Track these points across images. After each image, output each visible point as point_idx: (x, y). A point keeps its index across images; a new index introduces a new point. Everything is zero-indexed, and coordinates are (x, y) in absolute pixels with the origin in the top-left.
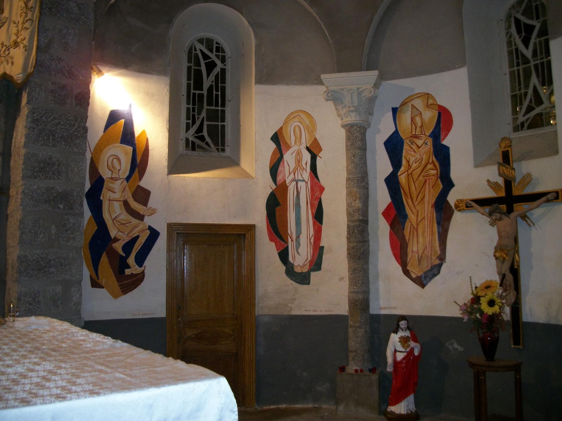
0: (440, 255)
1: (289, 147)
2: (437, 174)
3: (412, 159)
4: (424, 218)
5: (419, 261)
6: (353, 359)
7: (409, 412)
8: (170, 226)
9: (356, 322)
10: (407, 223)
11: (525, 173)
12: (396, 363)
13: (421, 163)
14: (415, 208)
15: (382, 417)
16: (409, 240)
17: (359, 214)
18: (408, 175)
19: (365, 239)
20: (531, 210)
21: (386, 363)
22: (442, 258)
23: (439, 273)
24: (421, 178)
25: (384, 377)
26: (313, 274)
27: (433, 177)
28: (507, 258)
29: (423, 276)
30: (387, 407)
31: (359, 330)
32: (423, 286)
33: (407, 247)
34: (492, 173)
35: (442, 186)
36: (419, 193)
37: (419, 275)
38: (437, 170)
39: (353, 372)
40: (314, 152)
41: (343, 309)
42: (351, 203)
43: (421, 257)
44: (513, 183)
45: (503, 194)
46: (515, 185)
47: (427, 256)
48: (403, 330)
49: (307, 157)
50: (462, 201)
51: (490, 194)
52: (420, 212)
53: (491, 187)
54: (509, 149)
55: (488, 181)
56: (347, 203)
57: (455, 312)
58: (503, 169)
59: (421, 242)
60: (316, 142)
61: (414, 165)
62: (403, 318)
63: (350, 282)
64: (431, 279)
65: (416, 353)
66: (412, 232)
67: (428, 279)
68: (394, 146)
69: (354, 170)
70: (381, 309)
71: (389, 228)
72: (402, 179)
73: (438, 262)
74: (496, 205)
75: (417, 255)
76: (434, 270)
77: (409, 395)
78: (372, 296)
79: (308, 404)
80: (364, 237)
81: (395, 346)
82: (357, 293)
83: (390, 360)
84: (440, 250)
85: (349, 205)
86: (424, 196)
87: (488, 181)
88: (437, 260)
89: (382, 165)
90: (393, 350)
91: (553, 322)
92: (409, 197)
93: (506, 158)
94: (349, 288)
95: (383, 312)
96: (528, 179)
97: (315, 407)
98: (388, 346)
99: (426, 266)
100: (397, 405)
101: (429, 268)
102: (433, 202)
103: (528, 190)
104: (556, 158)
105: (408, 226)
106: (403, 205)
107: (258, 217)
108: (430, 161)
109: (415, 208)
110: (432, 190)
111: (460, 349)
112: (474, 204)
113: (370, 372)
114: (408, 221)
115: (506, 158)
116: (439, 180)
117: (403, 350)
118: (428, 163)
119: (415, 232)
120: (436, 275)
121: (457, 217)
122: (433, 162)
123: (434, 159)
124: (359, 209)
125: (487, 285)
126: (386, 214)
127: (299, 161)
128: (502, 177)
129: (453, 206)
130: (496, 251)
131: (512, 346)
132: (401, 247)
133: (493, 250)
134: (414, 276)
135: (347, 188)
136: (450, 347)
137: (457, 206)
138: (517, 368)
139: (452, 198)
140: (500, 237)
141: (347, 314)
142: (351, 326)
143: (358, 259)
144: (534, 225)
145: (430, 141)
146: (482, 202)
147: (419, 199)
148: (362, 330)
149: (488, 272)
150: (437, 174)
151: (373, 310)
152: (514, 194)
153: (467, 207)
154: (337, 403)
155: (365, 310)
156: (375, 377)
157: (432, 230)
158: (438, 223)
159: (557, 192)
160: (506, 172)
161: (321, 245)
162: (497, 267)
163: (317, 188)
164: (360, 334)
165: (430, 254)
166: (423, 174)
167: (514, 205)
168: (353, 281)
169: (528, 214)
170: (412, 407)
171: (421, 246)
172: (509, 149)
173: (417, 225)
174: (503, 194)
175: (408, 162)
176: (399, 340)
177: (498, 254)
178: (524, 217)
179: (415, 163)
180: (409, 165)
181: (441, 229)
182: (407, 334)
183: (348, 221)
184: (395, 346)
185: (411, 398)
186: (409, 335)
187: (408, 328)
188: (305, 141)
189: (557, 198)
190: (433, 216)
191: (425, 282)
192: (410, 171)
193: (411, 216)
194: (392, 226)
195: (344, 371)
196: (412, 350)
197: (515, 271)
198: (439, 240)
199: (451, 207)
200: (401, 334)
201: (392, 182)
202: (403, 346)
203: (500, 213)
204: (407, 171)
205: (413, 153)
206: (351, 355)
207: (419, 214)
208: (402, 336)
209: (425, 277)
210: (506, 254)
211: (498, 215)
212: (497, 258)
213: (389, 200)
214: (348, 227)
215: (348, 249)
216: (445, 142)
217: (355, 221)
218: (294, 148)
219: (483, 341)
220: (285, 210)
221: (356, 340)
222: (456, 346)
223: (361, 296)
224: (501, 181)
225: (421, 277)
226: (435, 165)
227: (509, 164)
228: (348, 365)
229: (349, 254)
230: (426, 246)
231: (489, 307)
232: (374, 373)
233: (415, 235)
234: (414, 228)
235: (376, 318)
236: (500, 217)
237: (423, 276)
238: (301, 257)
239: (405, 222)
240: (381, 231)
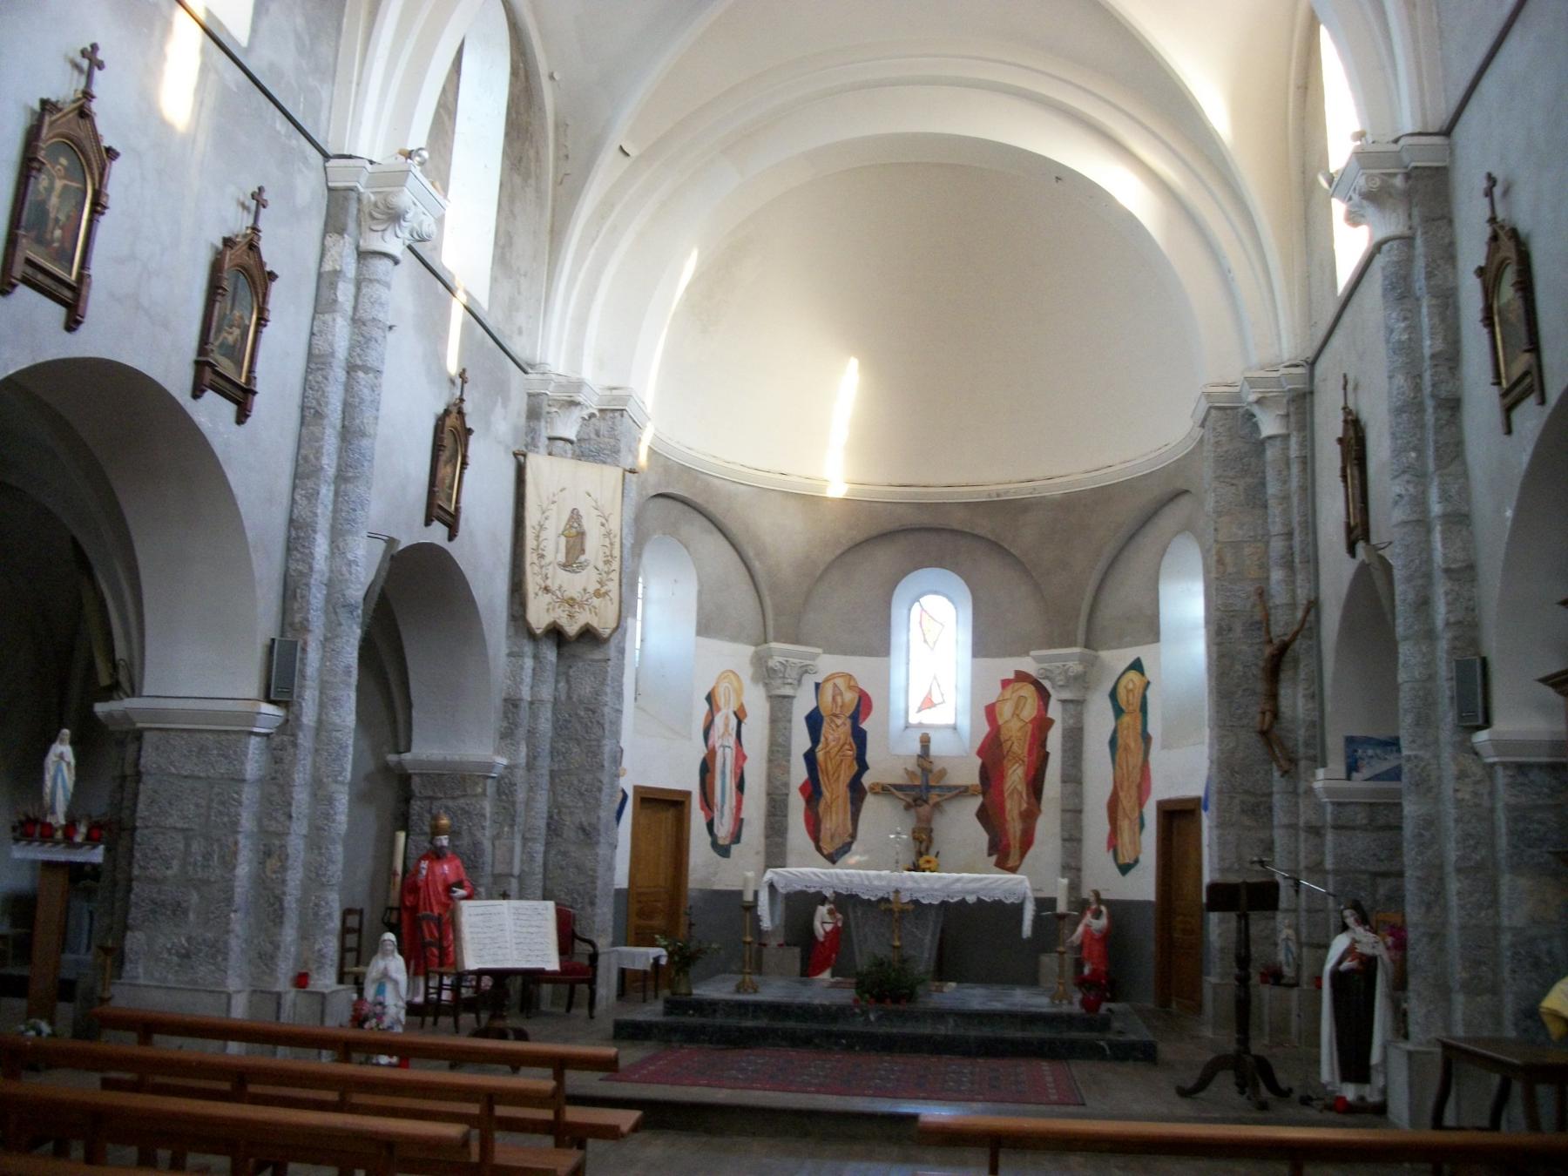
1: (719, 710)
8: (637, 789)
22: (853, 836)
26: (734, 848)
40: (740, 716)
49: (734, 721)
52: (835, 791)
59: (834, 821)
60: (742, 708)
68: (814, 722)
72: (820, 755)
89: (801, 740)
99: (838, 843)
107: (692, 784)
126: (803, 789)
127: (727, 725)
137: (872, 789)
139: (867, 780)
140: (919, 819)
145: (849, 722)
163: (740, 757)
188: (734, 706)
193: (826, 793)
201: (810, 758)
216: (864, 726)
218: (723, 711)
220: (713, 777)
238: (724, 830)
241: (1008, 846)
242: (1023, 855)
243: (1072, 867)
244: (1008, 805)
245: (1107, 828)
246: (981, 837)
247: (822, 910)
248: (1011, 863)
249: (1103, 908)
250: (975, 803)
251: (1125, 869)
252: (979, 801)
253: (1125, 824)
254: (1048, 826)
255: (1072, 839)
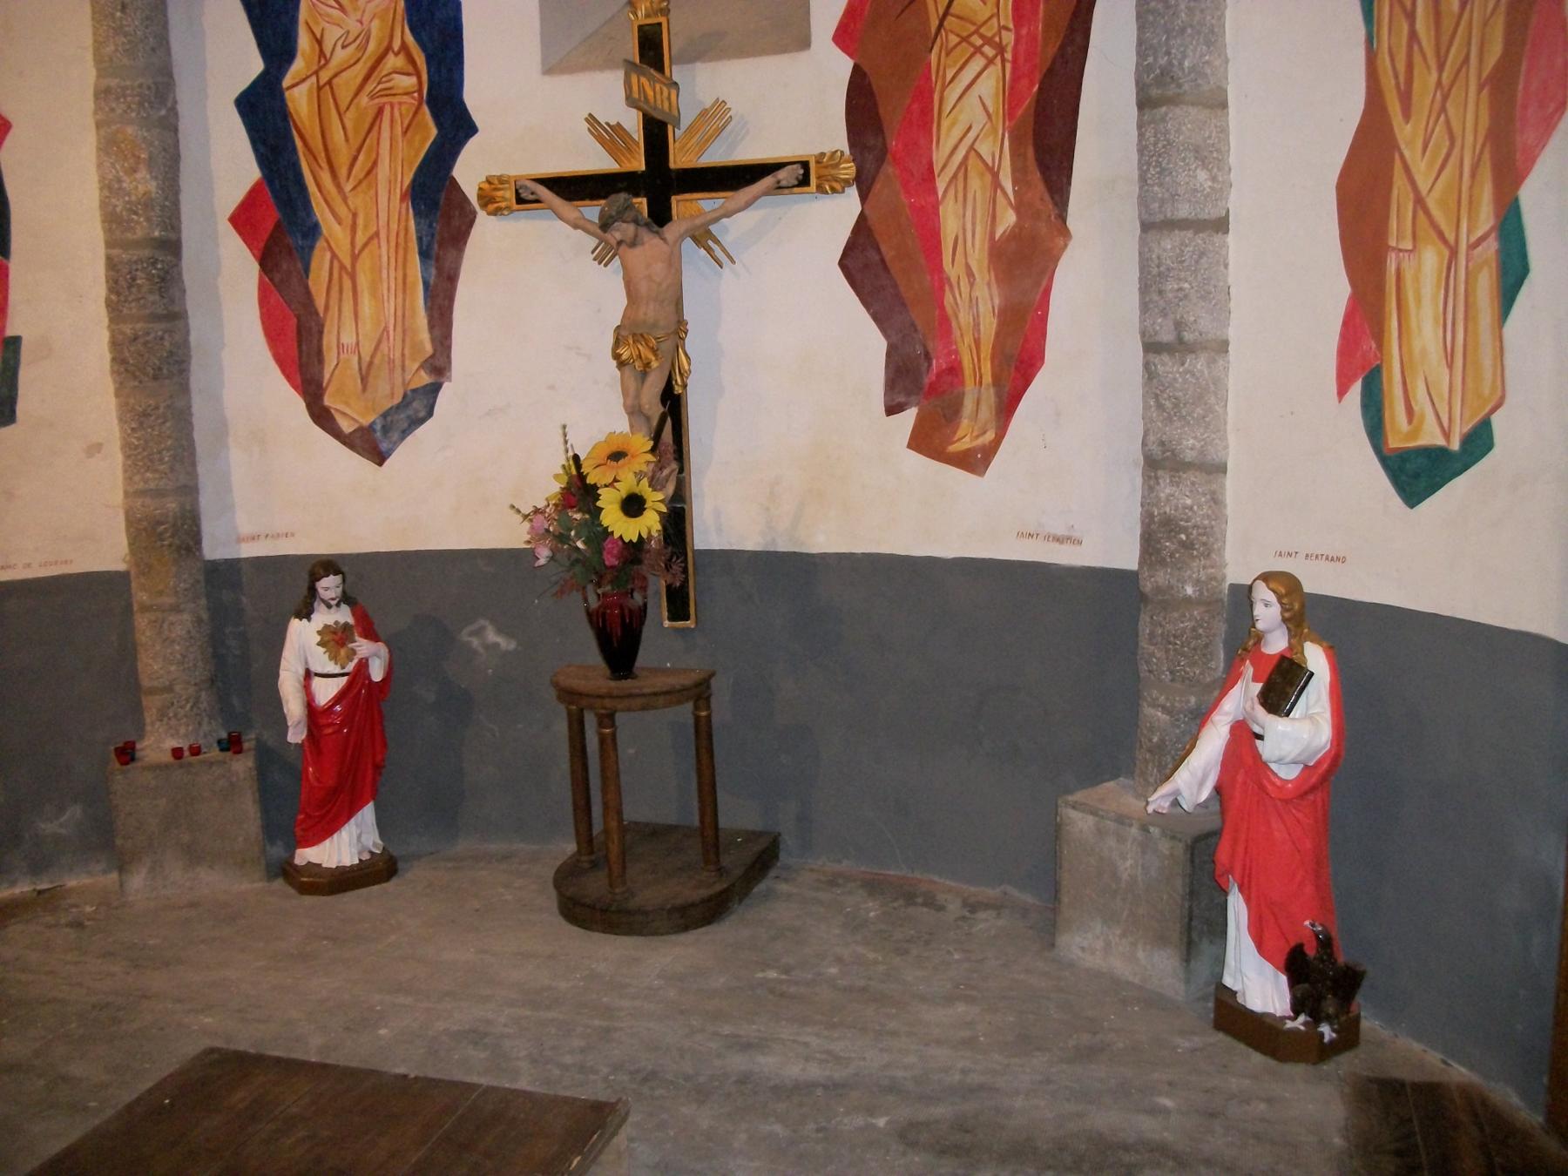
0: (432, 357)
2: (420, 91)
3: (332, 35)
4: (377, 234)
5: (364, 380)
6: (162, 714)
7: (366, 857)
9: (160, 593)
10: (316, 253)
11: (708, 103)
12: (314, 713)
13: (363, 48)
14: (345, 199)
15: (279, 884)
16: (327, 308)
17: (148, 219)
18: (319, 88)
19: (176, 309)
20: (728, 215)
21: (282, 719)
22: (439, 366)
23: (430, 414)
24: (364, 99)
25: (270, 758)
27: (405, 99)
28: (655, 364)
29: (378, 427)
30: (292, 856)
31: (172, 618)
32: (380, 458)
33: (321, 333)
34: (606, 95)
35: (434, 132)
36: (359, 150)
37: (365, 422)
38: (419, 78)
39: (167, 758)
41: (109, 551)
42: (120, 181)
43: (371, 364)
44: (670, 128)
45: (639, 164)
46: (676, 137)
47: (391, 362)
48: (329, 607)
50: (502, 180)
51: (598, 161)
52: (361, 214)
53: (600, 139)
54: (662, 20)
55: (591, 120)
56: (102, 179)
57: (514, 535)
58: (641, 88)
59: (367, 315)
61: (340, 56)
62: (328, 565)
63: (127, 457)
64: (405, 433)
65: (377, 674)
66: (335, 289)
67: (395, 436)
69: (125, 61)
70: (240, 540)
71: (255, 267)
72: (299, 99)
73: (425, 379)
74: (623, 196)
75: (356, 359)
76: (415, 404)
77: (361, 807)
78: (206, 502)
79: (13, 883)
80: (172, 301)
81: (309, 662)
82: (159, 493)
83: (294, 708)
84: (433, 340)
85: (110, 188)
86: (375, 164)
87: (591, 120)
88: (422, 373)
90: (302, 672)
91: (783, 547)
92: (324, 165)
93: (651, 49)
94: (129, 479)
95: (248, 551)
96: (716, 118)
97: (40, 892)
98: (283, 663)
99: (386, 393)
100: (327, 842)
101: (398, 399)
102: (407, 181)
103: (717, 155)
104: (803, 56)
105: (320, 264)
106: (303, 188)
108: (397, 45)
109: (345, 199)
110: (400, 143)
111: (506, 644)
112: (543, 192)
113: (222, 750)
114: (321, 244)
115: (651, 49)
116: (426, 109)
117: (337, 670)
118: (389, 48)
119: (347, 283)
120: (422, 421)
121: (486, 229)
122: (404, 47)
123: (410, 39)
124: (148, 204)
125: (614, 449)
126: (243, 220)
128: (638, 108)
129: (472, 196)
130: (617, 343)
131: (667, 623)
132: (299, 332)
133: (610, 340)
134: (347, 427)
135: (98, 125)
136: (475, 642)
137: (486, 199)
138: (700, 693)
139: (469, 171)
141: (121, 567)
142: (145, 609)
143: (155, 378)
144: (733, 262)
146: (572, 188)
147: (359, 170)
148: (186, 617)
149: (599, 413)
150: (420, 91)
151: (214, 550)
152: (672, 165)
153: (520, 200)
154: (122, 864)
155: (188, 549)
156: (242, 765)
157: (405, 276)
158: (424, 254)
159: (805, 165)
160: (650, 93)
161: (10, 332)
162: (625, 393)
164: (179, 631)
165: (398, 354)
166: (369, 87)
167: (674, 199)
168: (139, 456)
169: (713, 228)
170: (373, 840)
171: (367, 326)
172: (662, 20)
173: (355, 258)
174: (639, 164)
175: (319, 42)
176: (318, 638)
177: (625, 353)
178: (703, 237)
179: (344, 47)
180: (322, 53)
181: (433, 271)
182: (344, 615)
183: (109, 244)
184: (309, 662)
185: (368, 813)
186: (351, 620)
187: (346, 599)
189: (804, 181)
190: (407, 230)
191: (384, 446)
192: (325, 76)
194: (266, 261)
195: (133, 759)
196: (363, 665)
197: (673, 402)
198: (429, 309)
199: (465, 199)
200: (323, 617)
201: (262, 108)
202: (334, 657)
203: (636, 222)
204: (316, 73)
205: (336, 13)
206: (151, 704)
207: (360, 221)
208: (326, 627)
209: (386, 430)
210: (654, 351)
211: (630, 229)
212: (621, 364)
213: (251, 172)
214: (111, 264)
215: (115, 344)
217: (137, 244)
219: (600, 623)
221: (166, 651)
222: (492, 636)
223: (172, 505)
224: (632, 122)
225: (371, 427)
226: (412, 61)
227: (661, 69)
228: (142, 737)
229: (119, 361)
230: (386, 329)
231: (620, 514)
232: (239, 751)
233: (348, 293)
234: (342, 267)
235: (225, 574)
236: (636, 236)
237: (378, 427)
239: (312, 248)
240: (226, 278)
241: (954, 370)
242: (1007, 406)
243: (1173, 462)
244: (950, 222)
245: (1338, 290)
246: (864, 346)
247: (303, 640)
248: (965, 439)
249: (1316, 658)
250: (834, 216)
251: (1417, 474)
252: (846, 208)
253: (1421, 272)
254: (1091, 291)
255: (1175, 346)
